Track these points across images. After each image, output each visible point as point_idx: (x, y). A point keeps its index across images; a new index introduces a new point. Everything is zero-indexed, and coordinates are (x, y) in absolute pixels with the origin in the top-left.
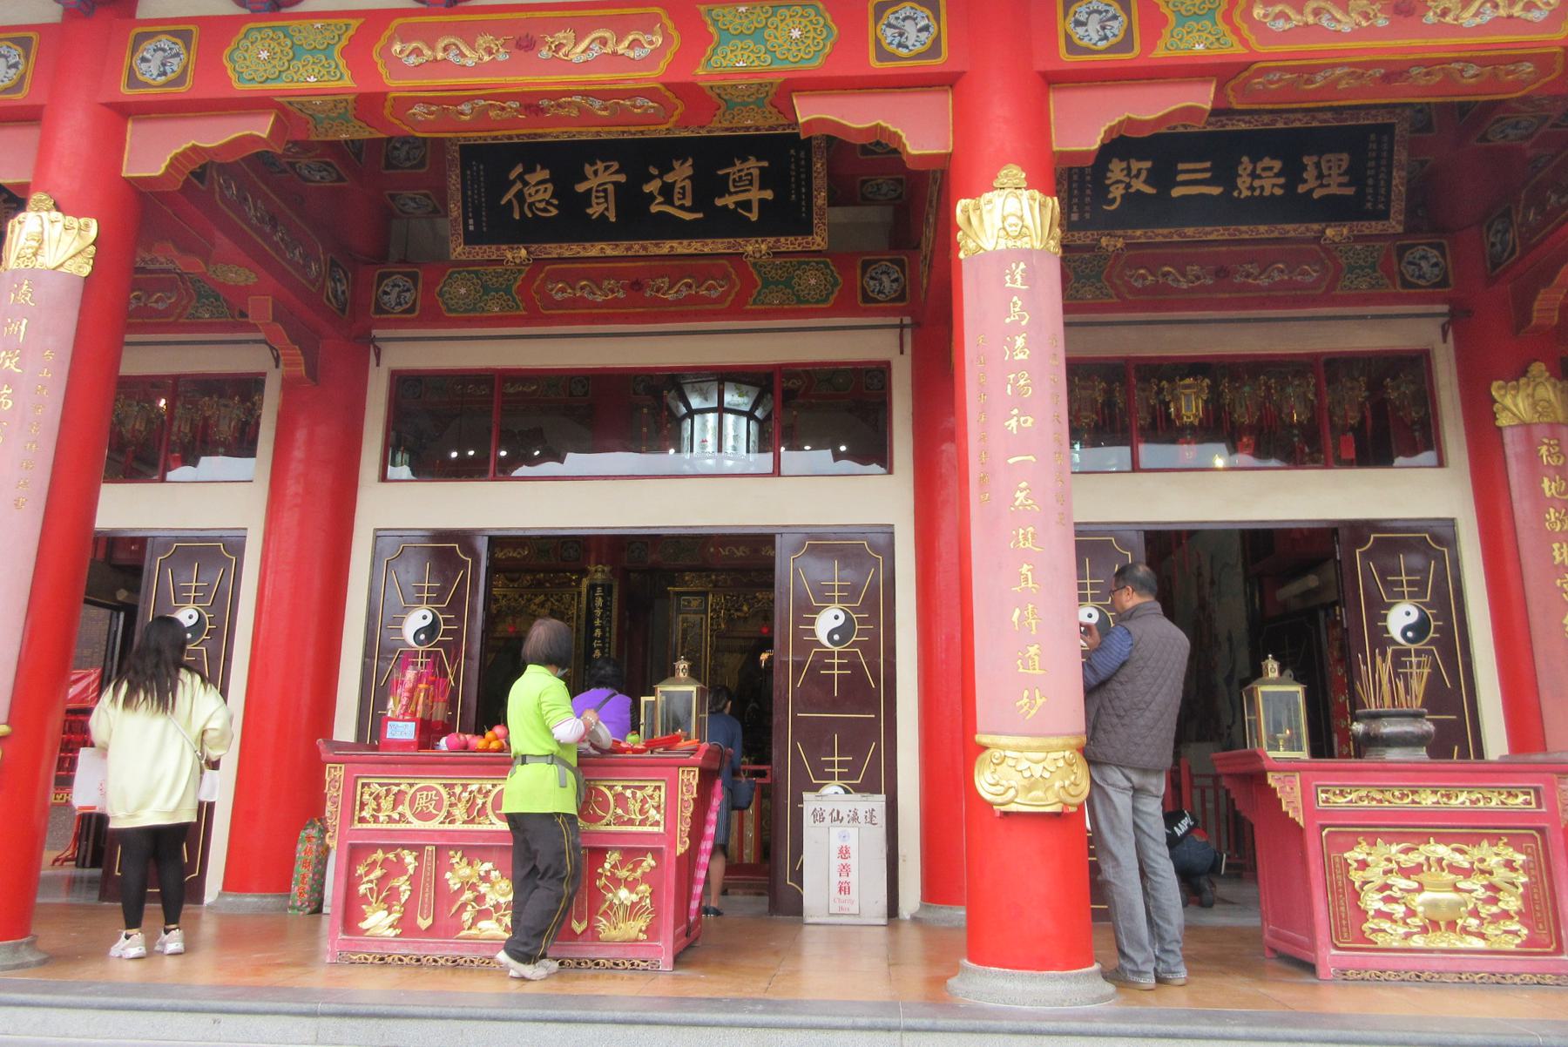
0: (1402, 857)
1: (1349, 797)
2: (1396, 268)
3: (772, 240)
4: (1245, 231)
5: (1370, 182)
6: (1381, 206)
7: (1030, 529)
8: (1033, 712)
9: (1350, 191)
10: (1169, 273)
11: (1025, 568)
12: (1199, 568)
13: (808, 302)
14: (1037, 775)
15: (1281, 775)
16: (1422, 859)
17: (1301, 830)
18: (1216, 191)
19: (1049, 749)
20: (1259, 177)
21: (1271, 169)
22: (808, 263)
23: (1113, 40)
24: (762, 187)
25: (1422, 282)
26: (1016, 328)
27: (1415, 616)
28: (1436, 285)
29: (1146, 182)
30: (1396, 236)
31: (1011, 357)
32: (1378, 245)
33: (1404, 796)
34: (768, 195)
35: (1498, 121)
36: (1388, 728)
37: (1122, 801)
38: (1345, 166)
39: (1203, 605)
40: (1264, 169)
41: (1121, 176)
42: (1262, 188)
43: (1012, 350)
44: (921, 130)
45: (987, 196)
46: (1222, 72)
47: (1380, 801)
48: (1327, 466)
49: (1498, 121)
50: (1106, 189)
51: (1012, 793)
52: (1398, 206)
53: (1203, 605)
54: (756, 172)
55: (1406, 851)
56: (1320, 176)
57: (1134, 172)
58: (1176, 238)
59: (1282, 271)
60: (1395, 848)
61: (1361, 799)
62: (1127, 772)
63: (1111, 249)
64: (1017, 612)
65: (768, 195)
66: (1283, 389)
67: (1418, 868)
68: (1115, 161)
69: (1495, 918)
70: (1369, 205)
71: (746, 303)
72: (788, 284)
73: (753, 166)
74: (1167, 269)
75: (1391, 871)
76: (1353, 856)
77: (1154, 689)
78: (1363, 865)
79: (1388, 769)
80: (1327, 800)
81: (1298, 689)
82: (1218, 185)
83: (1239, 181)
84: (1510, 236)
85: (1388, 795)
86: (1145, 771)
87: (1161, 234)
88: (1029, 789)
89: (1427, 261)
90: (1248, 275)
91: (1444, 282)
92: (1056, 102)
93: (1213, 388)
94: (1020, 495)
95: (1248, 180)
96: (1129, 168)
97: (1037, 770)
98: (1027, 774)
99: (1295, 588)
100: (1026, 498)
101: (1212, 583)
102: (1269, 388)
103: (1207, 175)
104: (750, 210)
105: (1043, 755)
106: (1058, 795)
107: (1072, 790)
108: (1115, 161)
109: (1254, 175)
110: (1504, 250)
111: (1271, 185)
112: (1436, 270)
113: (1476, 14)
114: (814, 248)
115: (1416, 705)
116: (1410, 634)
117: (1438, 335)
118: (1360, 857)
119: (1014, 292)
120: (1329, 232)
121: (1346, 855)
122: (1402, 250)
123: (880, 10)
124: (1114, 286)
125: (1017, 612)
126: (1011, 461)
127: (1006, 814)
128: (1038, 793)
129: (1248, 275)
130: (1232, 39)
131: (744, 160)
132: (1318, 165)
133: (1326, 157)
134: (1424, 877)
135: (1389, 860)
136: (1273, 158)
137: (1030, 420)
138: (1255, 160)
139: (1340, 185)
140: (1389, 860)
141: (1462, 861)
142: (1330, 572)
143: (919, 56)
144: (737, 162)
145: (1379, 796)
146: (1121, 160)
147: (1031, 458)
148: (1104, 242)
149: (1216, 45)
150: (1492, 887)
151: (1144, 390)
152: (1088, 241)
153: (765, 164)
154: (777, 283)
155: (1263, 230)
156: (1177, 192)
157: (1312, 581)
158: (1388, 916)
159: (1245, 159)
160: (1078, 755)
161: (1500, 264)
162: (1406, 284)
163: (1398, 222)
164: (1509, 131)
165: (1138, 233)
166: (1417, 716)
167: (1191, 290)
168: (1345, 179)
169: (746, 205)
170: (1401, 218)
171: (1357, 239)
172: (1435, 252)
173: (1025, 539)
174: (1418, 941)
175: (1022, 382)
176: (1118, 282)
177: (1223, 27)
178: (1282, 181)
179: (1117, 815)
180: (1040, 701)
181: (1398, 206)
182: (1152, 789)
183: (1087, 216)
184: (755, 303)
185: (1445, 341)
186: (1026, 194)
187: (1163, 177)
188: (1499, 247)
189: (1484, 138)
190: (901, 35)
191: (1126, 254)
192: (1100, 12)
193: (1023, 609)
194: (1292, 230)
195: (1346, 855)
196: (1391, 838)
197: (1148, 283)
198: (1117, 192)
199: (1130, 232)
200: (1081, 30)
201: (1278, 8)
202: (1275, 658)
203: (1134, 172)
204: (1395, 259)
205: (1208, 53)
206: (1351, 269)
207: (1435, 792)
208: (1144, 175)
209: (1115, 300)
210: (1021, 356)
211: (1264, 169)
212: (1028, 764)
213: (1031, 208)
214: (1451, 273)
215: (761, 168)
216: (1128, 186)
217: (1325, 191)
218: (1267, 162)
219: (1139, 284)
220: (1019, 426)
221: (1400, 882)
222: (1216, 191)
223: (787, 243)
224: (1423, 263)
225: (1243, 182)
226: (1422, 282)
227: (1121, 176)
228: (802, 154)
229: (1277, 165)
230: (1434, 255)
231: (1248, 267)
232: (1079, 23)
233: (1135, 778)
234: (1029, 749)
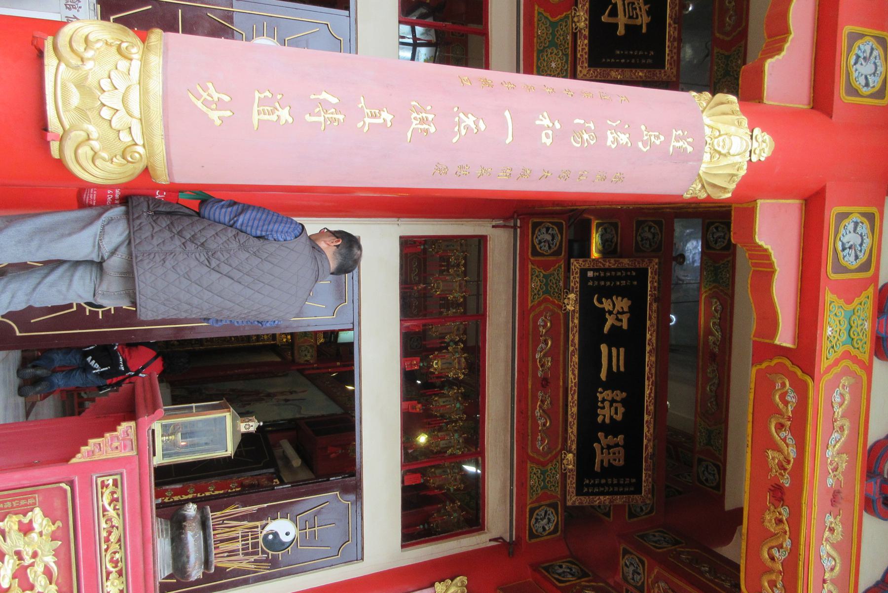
0: (39, 568)
1: (110, 509)
2: (543, 503)
3: (586, 32)
4: (573, 398)
5: (603, 481)
6: (586, 490)
7: (432, 129)
8: (199, 104)
9: (597, 468)
10: (547, 344)
11: (387, 116)
12: (295, 392)
13: (538, 59)
14: (104, 98)
15: (133, 436)
17: (67, 460)
18: (603, 375)
19: (145, 121)
20: (611, 406)
21: (616, 413)
22: (566, 62)
23: (841, 255)
24: (627, 26)
25: (533, 521)
26: (635, 136)
27: (285, 539)
28: (530, 529)
29: (613, 326)
31: (610, 128)
32: (559, 489)
33: (115, 563)
34: (621, 31)
35: (640, 560)
36: (192, 538)
37: (81, 244)
38: (616, 463)
39: (269, 395)
40: (616, 409)
41: (618, 308)
42: (603, 408)
43: (616, 129)
44: (784, 73)
45: (745, 121)
46: (804, 354)
47: (107, 540)
48: (403, 466)
49: (640, 560)
50: (609, 297)
51: (75, 61)
52: (585, 501)
53: (269, 395)
54: (638, 22)
55: (48, 572)
56: (609, 447)
57: (620, 316)
58: (571, 349)
59: (544, 424)
60: (50, 560)
61: (109, 520)
62: (123, 250)
63: (566, 301)
64: (334, 100)
65: (621, 31)
66: (456, 431)
68: (630, 303)
70: (587, 482)
71: (540, 6)
72: (553, 44)
73: (644, 20)
74: (550, 343)
75: (21, 558)
76: (37, 516)
77: (237, 275)
78: (26, 529)
79: (147, 543)
80: (104, 485)
81: (230, 451)
82: (607, 377)
83: (609, 392)
84: (570, 577)
85: (115, 547)
86: (129, 275)
87: (575, 338)
88: (81, 85)
89: (547, 523)
90: (543, 401)
91: (532, 535)
92: (794, 204)
93: (456, 382)
94: (470, 121)
95: (610, 398)
96: (623, 313)
97: (112, 99)
98: (106, 84)
99: (290, 451)
100: (467, 128)
101: (287, 400)
102: (456, 421)
103: (615, 369)
104: (610, 15)
105: (135, 109)
106: (73, 127)
107: (85, 152)
108: (630, 303)
109: (613, 401)
110: (559, 574)
111: (605, 414)
112: (541, 530)
113: (829, 555)
114: (579, 68)
115: (215, 562)
116: (271, 537)
117: (495, 535)
118: (36, 525)
119: (668, 137)
120: (570, 456)
121: (37, 510)
122: (554, 506)
123: (881, 41)
124: (539, 304)
125: (334, 100)
126: (507, 114)
127: (40, 54)
128: (75, 99)
129: (543, 401)
130: (832, 357)
131: (648, 13)
132: (617, 445)
133: (622, 450)
136: (624, 414)
137: (548, 142)
138: (623, 402)
139: (602, 461)
140: (35, 555)
142: (305, 475)
143: (848, 75)
144: (647, 7)
145: (113, 538)
146: (629, 307)
147: (509, 139)
148: (572, 296)
149: (829, 345)
151: (458, 329)
152: (572, 284)
153: (644, 30)
154: (553, 34)
155: (573, 410)
156: (604, 348)
157: (297, 462)
159: (624, 395)
160: (140, 167)
161: (548, 571)
162: (532, 511)
163: (574, 502)
164: (632, 569)
165: (576, 321)
166: (207, 563)
167: (535, 360)
168: (606, 464)
169: (614, 13)
170: (577, 504)
171: (564, 476)
172: (552, 529)
173: (423, 121)
175: (586, 136)
176: (542, 307)
177: (840, 350)
178: (607, 421)
179: (63, 236)
180: (215, 116)
181: (585, 501)
182: (104, 286)
183: (590, 283)
184: (539, 13)
185: (490, 540)
186: (743, 160)
187: (616, 338)
188: (560, 571)
189: (626, 552)
190: (865, 58)
191: (561, 313)
192: (861, 245)
193: (338, 109)
194: (573, 431)
195: (37, 510)
196: (63, 556)
197: (541, 329)
198: (607, 305)
199: (577, 315)
200: (851, 227)
201: (847, 397)
202: (259, 428)
203: (620, 316)
204: (548, 502)
205: (824, 338)
206: (543, 473)
208: (618, 324)
210: (610, 138)
211: (616, 409)
212: (122, 89)
213: (733, 165)
214: (538, 540)
215: (641, 26)
216: (610, 313)
217: (598, 451)
218: (621, 410)
219: (540, 322)
220: (542, 128)
222: (603, 375)
223: (583, 44)
224: (545, 521)
225: (608, 394)
226: (533, 521)
227: (618, 308)
228: (650, 61)
229: (619, 417)
230: (552, 527)
231: (548, 401)
232: (856, 224)
233: (116, 263)
234: (144, 92)
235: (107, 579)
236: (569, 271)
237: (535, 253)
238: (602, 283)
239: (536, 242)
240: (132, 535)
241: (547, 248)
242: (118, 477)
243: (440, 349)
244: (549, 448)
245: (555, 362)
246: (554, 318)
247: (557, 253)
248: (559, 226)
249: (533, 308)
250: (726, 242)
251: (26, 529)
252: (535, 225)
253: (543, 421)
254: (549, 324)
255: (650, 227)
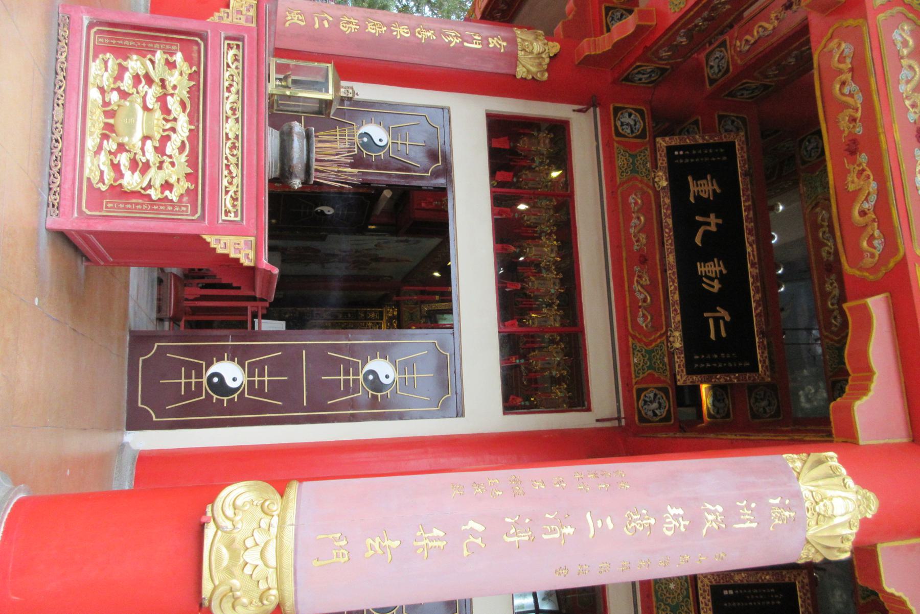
16: (174, 114)
30: (675, 380)
59: (645, 300)
60: (185, 95)
67: (166, 110)
69: (116, 167)
74: (642, 218)
75: (163, 86)
76: (179, 57)
90: (640, 277)
91: (642, 419)
124: (628, 181)
134: (158, 114)
135: (175, 87)
141: (171, 148)
150: (146, 166)
158: (119, 77)
172: (664, 414)
174: (94, 94)
185: (598, 420)
207: (237, 137)
209: (618, 181)
219: (631, 200)
221: (152, 93)
235: (227, 122)
236: (655, 151)
237: (618, 134)
238: (687, 161)
239: (618, 124)
240: (249, 129)
241: (629, 131)
242: (240, 43)
243: (534, 238)
244: (652, 327)
245: (649, 238)
246: (644, 195)
247: (642, 135)
248: (641, 112)
249: (622, 184)
250: (820, 150)
251: (171, 65)
252: (617, 110)
253: (642, 296)
254: (639, 201)
255: (733, 122)
